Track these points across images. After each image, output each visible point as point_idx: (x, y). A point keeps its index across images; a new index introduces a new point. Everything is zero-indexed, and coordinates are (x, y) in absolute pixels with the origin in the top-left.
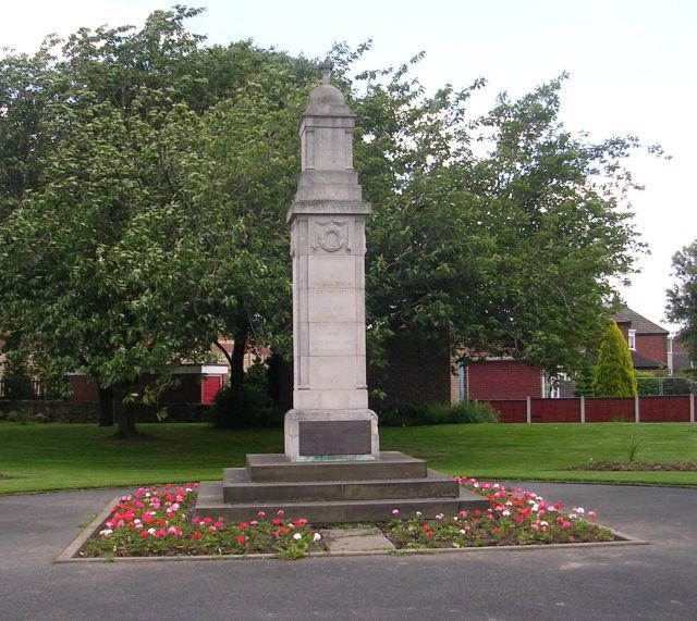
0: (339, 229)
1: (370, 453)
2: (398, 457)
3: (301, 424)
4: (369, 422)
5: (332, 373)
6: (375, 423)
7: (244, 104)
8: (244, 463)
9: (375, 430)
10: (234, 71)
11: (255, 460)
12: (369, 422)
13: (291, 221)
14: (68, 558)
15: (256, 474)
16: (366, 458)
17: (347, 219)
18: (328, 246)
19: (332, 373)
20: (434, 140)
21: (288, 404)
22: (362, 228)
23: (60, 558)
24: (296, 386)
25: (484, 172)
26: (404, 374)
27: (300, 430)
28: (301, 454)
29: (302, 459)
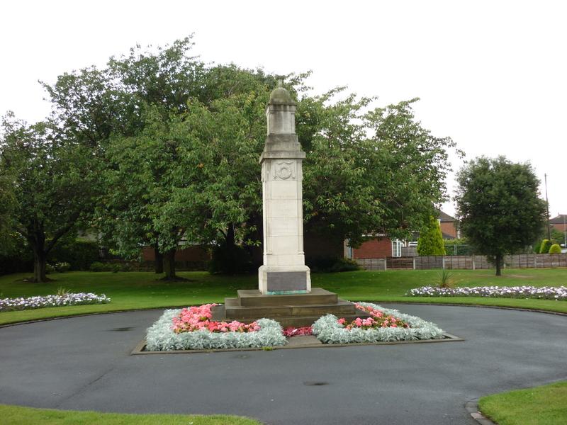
0: (288, 166)
1: (306, 289)
2: (322, 292)
3: (268, 274)
4: (305, 272)
5: (284, 247)
6: (309, 273)
7: (228, 105)
8: (236, 294)
9: (309, 277)
10: (222, 84)
11: (242, 294)
12: (305, 272)
13: (262, 162)
14: (139, 352)
15: (244, 302)
16: (304, 292)
17: (291, 161)
18: (283, 176)
19: (284, 247)
20: (341, 131)
21: (261, 263)
22: (300, 166)
23: (134, 352)
24: (265, 253)
25: (370, 143)
26: (325, 239)
27: (268, 277)
28: (268, 290)
29: (269, 293)
